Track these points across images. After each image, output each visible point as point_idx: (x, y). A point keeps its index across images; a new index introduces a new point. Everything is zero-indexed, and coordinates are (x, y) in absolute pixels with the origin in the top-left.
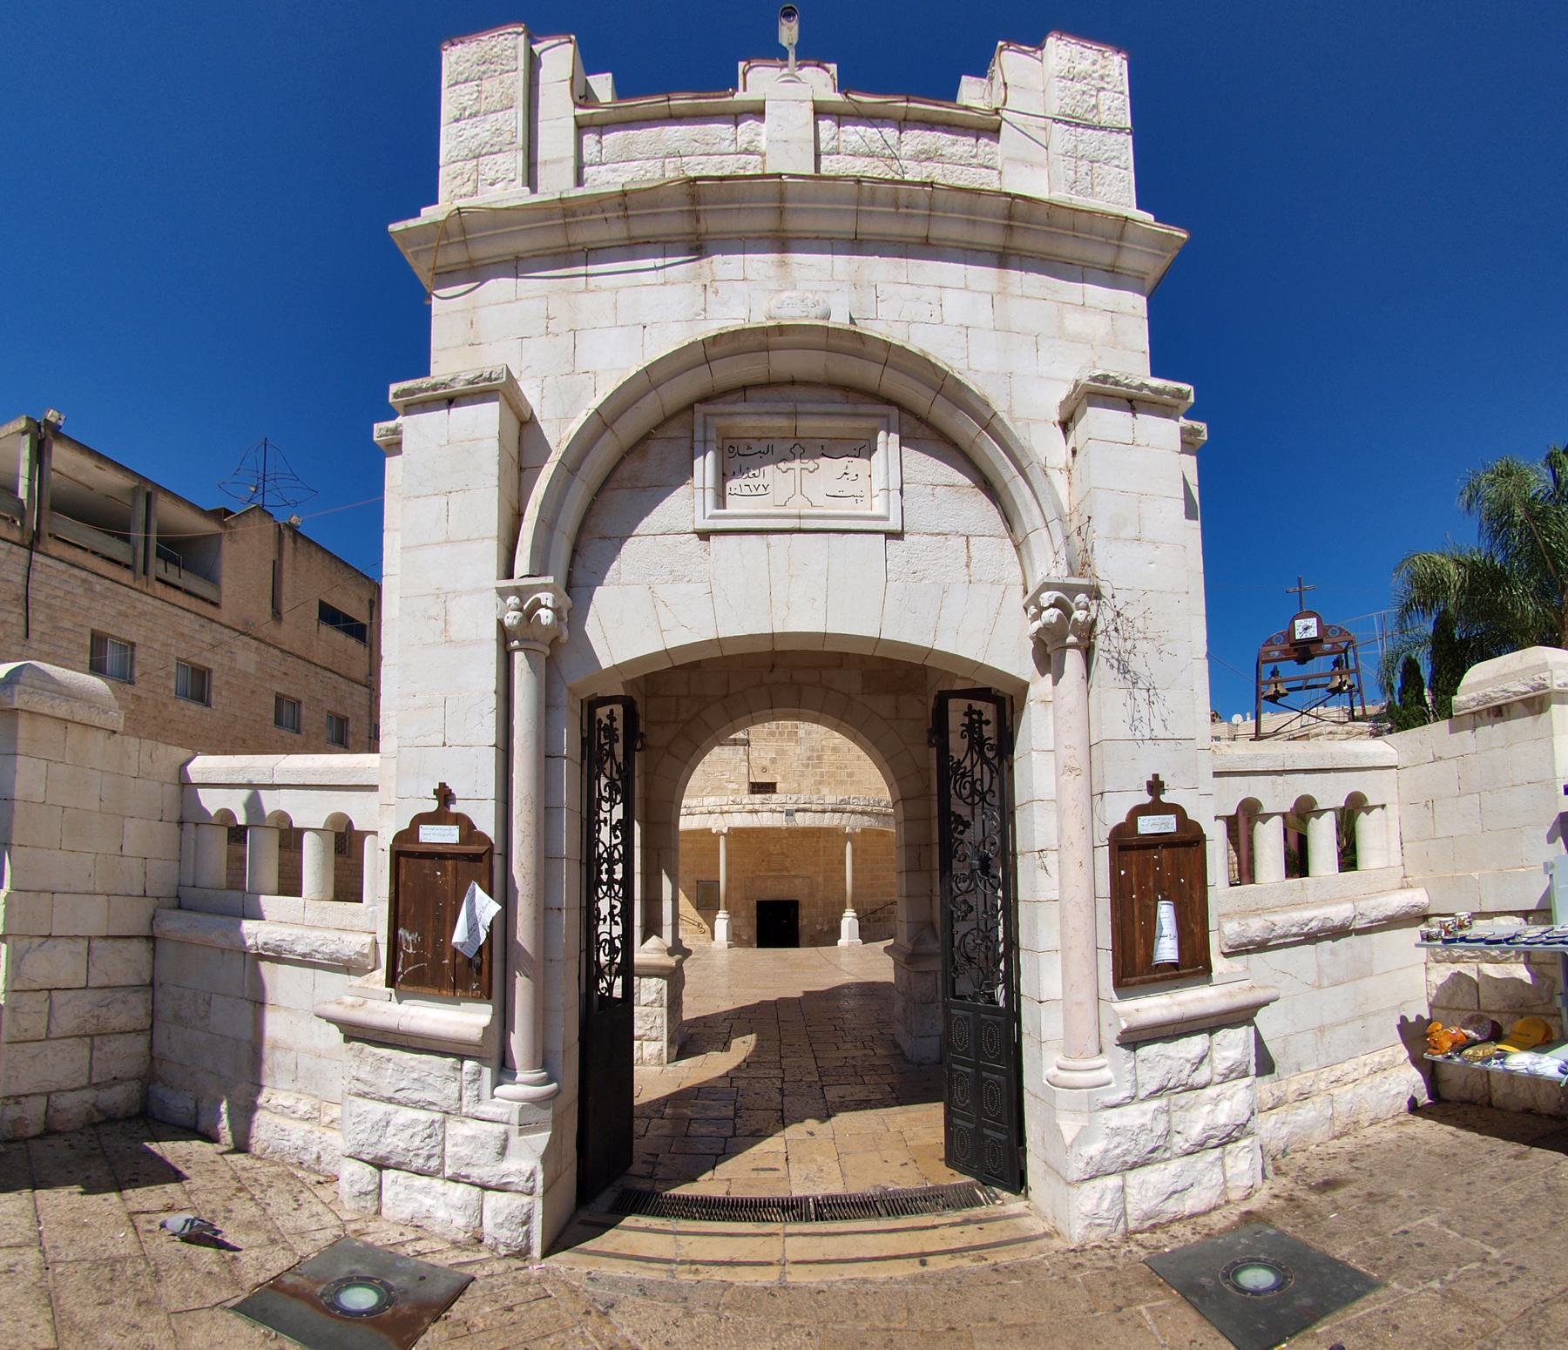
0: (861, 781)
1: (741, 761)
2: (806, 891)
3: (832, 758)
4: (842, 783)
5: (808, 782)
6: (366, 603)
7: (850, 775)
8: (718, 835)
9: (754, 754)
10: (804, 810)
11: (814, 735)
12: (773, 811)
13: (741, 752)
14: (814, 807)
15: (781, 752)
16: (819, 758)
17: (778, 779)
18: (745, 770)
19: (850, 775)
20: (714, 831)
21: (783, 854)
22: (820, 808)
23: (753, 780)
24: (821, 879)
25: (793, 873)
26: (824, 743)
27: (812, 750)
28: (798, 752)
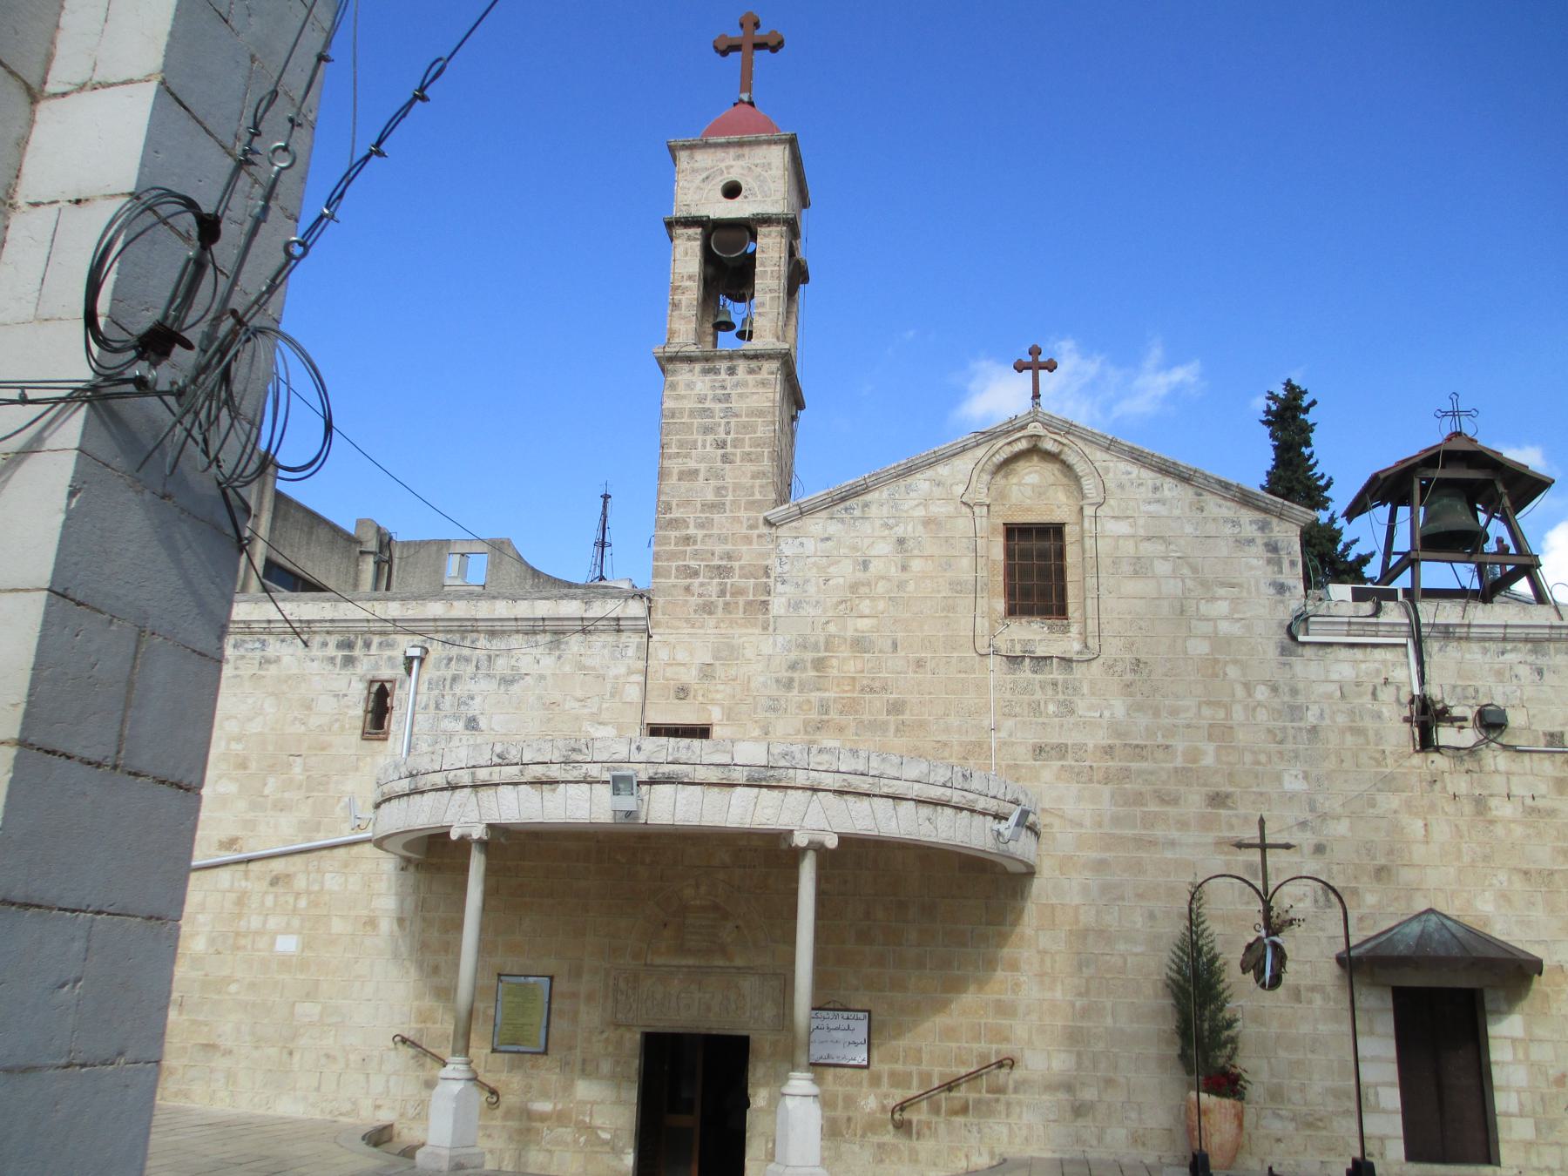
0: (921, 724)
1: (630, 673)
3: (851, 667)
4: (875, 726)
5: (786, 726)
7: (896, 708)
8: (464, 843)
9: (660, 654)
10: (669, 780)
11: (809, 610)
12: (589, 781)
13: (631, 652)
14: (701, 774)
15: (728, 652)
16: (819, 664)
17: (714, 716)
18: (634, 693)
21: (716, 907)
22: (714, 775)
25: (739, 962)
26: (832, 628)
27: (804, 647)
28: (767, 648)
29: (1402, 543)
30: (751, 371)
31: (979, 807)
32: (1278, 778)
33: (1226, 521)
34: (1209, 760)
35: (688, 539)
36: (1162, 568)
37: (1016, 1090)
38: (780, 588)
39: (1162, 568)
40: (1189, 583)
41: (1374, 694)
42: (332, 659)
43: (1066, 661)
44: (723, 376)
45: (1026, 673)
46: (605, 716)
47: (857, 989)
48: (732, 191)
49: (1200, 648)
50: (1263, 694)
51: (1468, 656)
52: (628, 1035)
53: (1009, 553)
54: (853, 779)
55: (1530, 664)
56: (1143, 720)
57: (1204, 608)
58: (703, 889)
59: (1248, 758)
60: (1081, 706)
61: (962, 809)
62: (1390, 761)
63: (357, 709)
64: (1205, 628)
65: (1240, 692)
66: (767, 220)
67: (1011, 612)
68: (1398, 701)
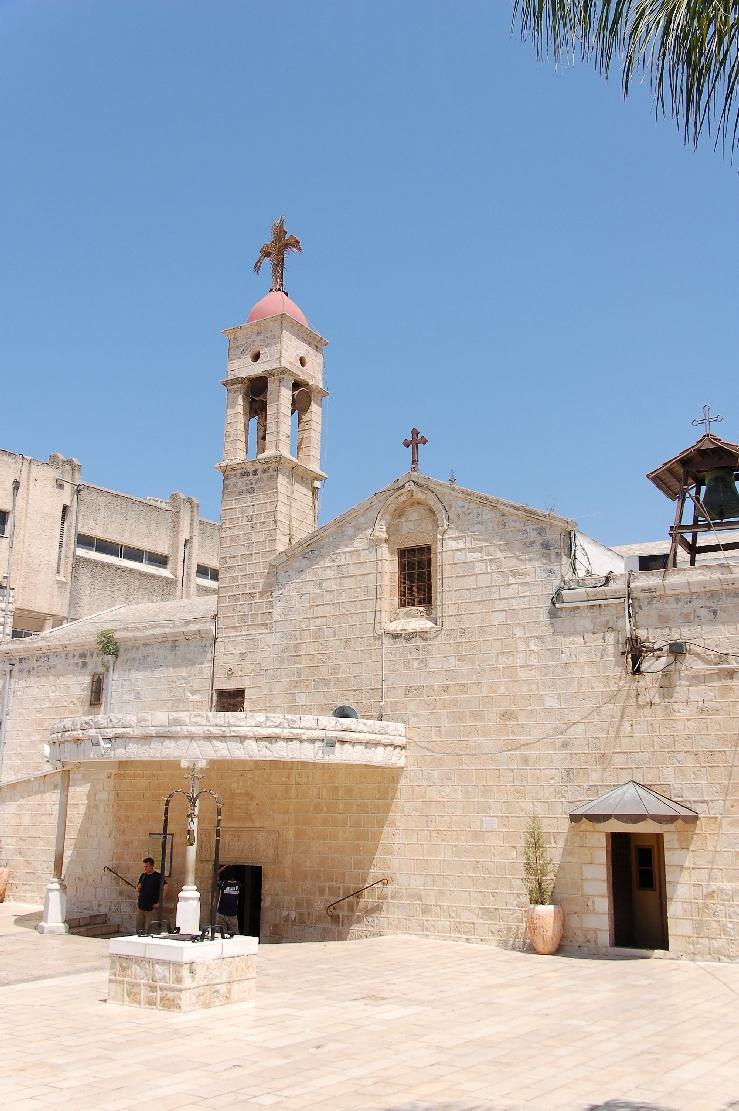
2: (271, 852)
4: (325, 682)
6: (10, 486)
19: (335, 669)
20: (184, 764)
21: (247, 794)
23: (218, 686)
24: (291, 834)
29: (688, 520)
30: (264, 471)
31: (304, 737)
32: (541, 698)
33: (519, 531)
34: (502, 690)
35: (234, 579)
36: (479, 568)
37: (393, 897)
38: (279, 604)
39: (479, 568)
40: (495, 576)
41: (604, 639)
42: (77, 663)
43: (422, 635)
44: (251, 477)
45: (401, 643)
46: (196, 687)
47: (313, 839)
48: (256, 357)
49: (499, 618)
50: (536, 645)
51: (666, 606)
52: (207, 866)
53: (402, 567)
54: (211, 729)
55: (709, 607)
56: (465, 667)
57: (505, 593)
58: (241, 783)
59: (525, 688)
60: (432, 664)
61: (291, 740)
62: (611, 684)
63: (87, 693)
64: (502, 605)
65: (522, 647)
66: (271, 373)
67: (403, 605)
68: (618, 642)
